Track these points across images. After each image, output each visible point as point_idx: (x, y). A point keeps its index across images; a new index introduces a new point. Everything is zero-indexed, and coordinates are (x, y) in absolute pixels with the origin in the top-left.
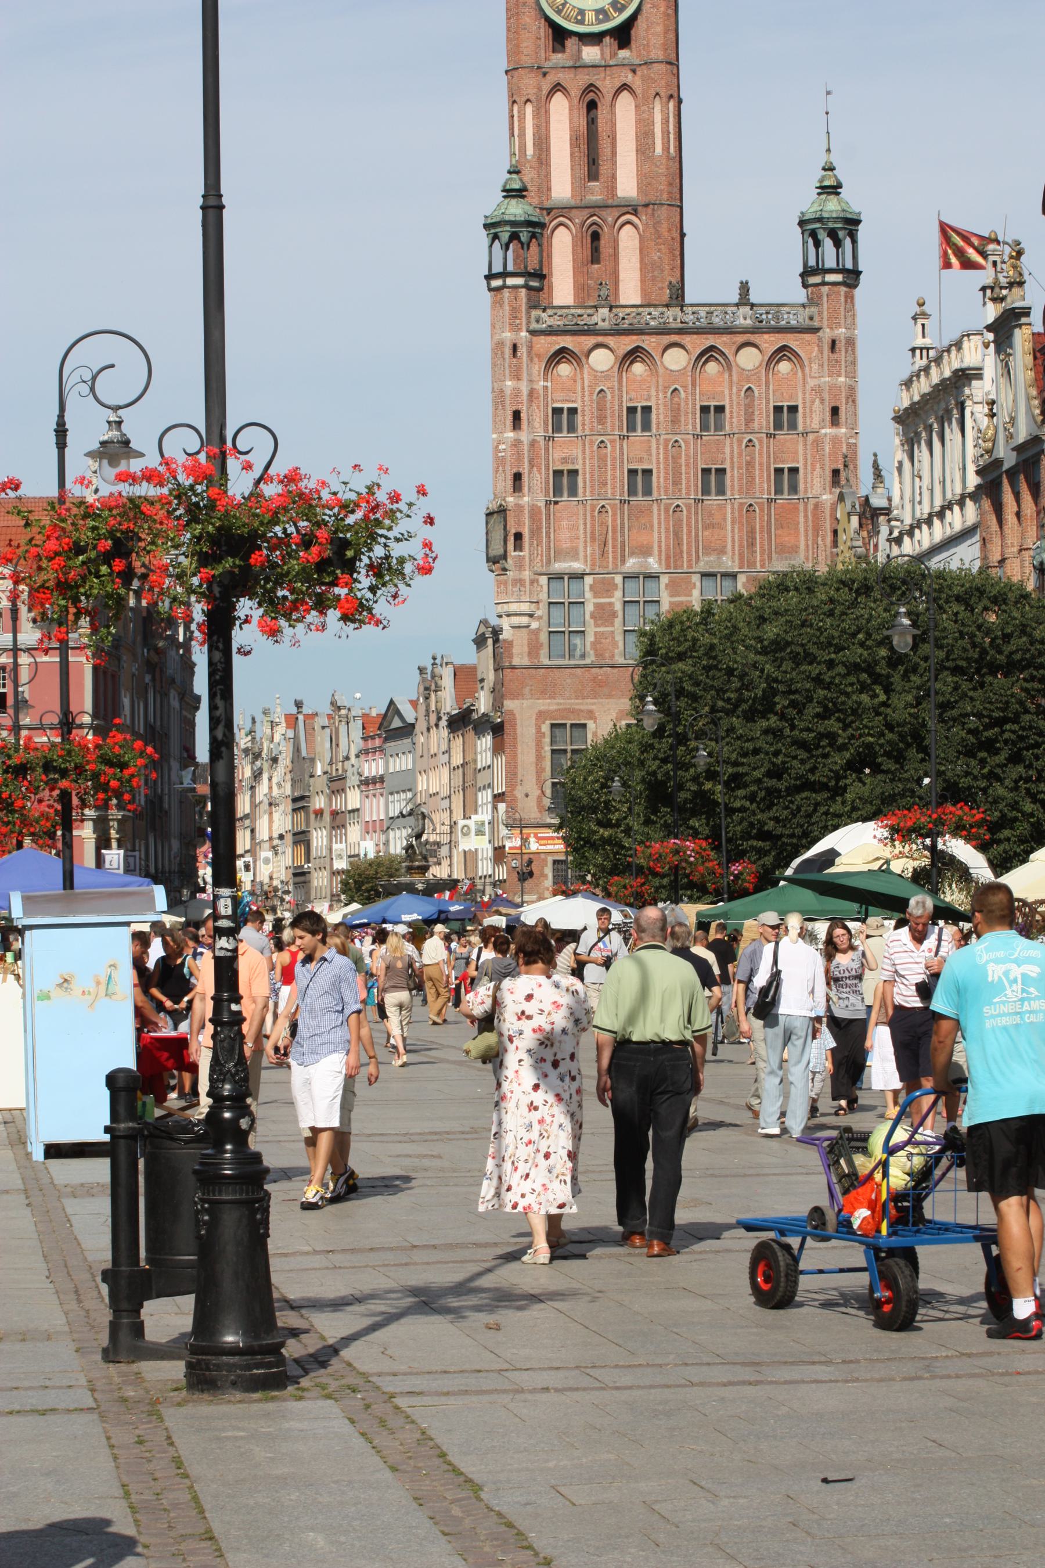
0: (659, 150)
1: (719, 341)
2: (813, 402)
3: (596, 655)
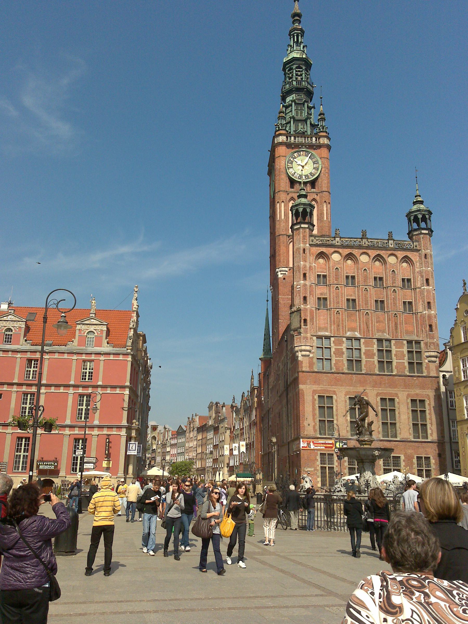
0: (325, 219)
1: (382, 253)
2: (418, 277)
3: (336, 369)
